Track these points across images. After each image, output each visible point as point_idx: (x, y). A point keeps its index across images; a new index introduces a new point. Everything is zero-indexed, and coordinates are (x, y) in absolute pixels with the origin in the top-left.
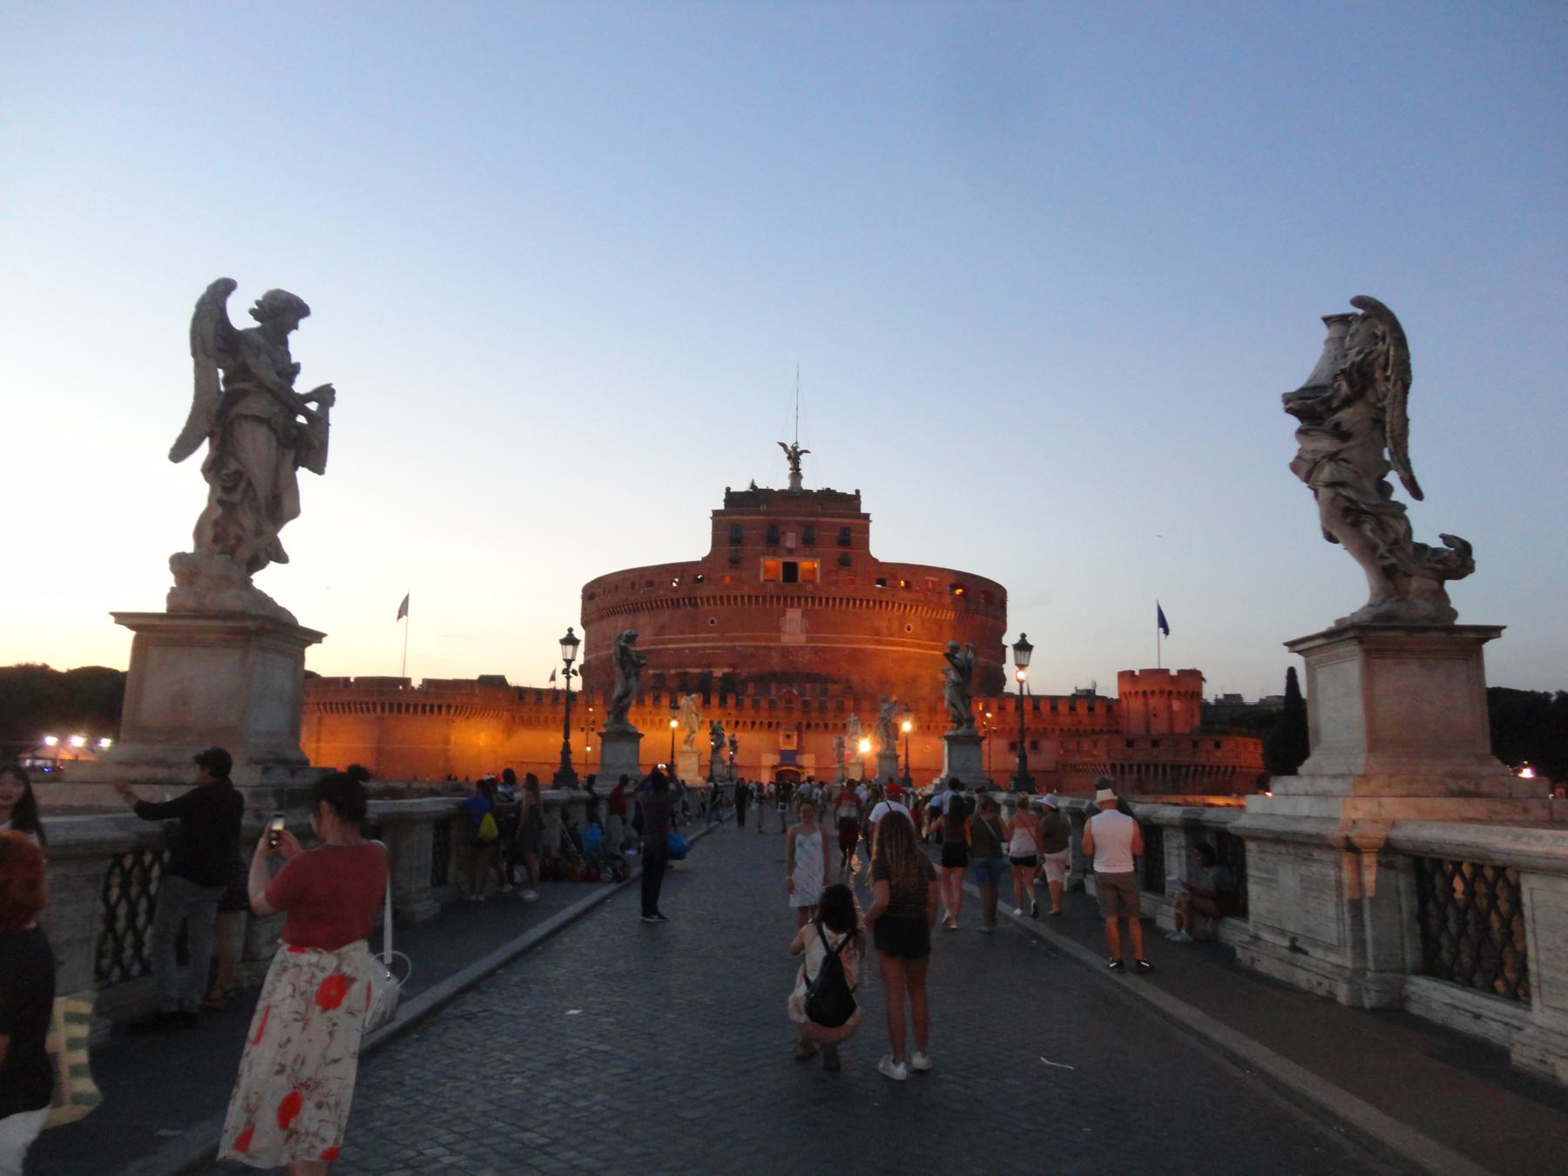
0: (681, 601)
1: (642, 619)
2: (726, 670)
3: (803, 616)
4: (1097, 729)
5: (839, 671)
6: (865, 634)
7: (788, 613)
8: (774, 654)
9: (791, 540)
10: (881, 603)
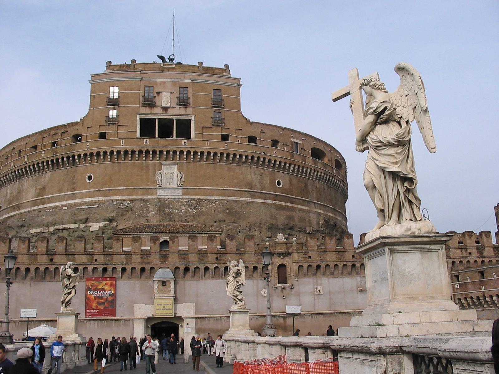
2: (102, 224)
3: (179, 170)
4: (487, 260)
5: (215, 222)
6: (240, 187)
7: (164, 167)
8: (151, 207)
9: (166, 100)
10: (253, 157)
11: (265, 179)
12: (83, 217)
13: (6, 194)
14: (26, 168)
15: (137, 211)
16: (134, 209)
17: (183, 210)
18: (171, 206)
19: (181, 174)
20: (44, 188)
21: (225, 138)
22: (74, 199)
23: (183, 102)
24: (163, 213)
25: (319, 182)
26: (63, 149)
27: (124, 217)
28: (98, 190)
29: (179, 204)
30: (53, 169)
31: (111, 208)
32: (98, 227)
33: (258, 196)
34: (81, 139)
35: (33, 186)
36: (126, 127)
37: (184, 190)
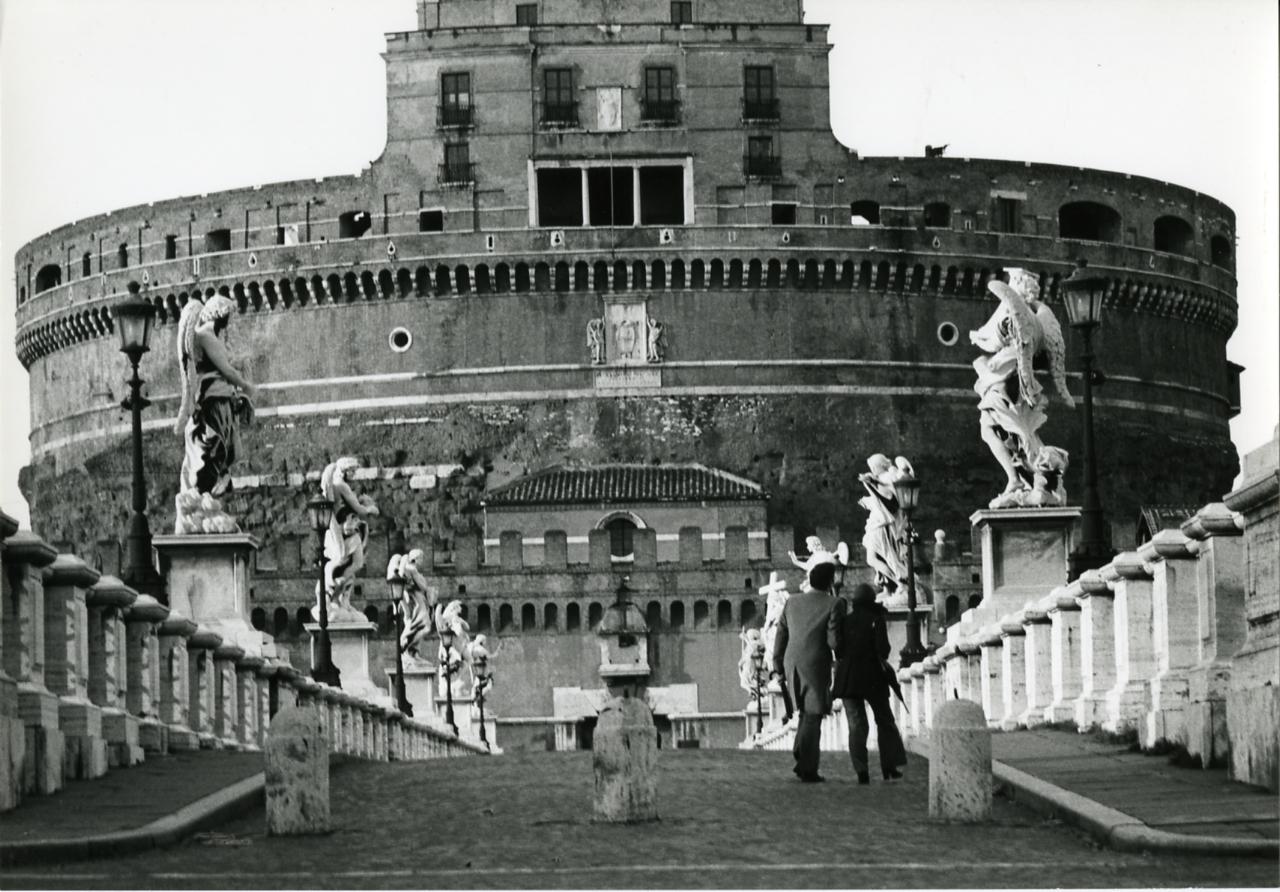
0: (309, 286)
2: (445, 471)
5: (757, 459)
12: (389, 451)
18: (631, 417)
19: (658, 325)
21: (784, 215)
26: (314, 254)
28: (430, 377)
30: (288, 305)
33: (881, 377)
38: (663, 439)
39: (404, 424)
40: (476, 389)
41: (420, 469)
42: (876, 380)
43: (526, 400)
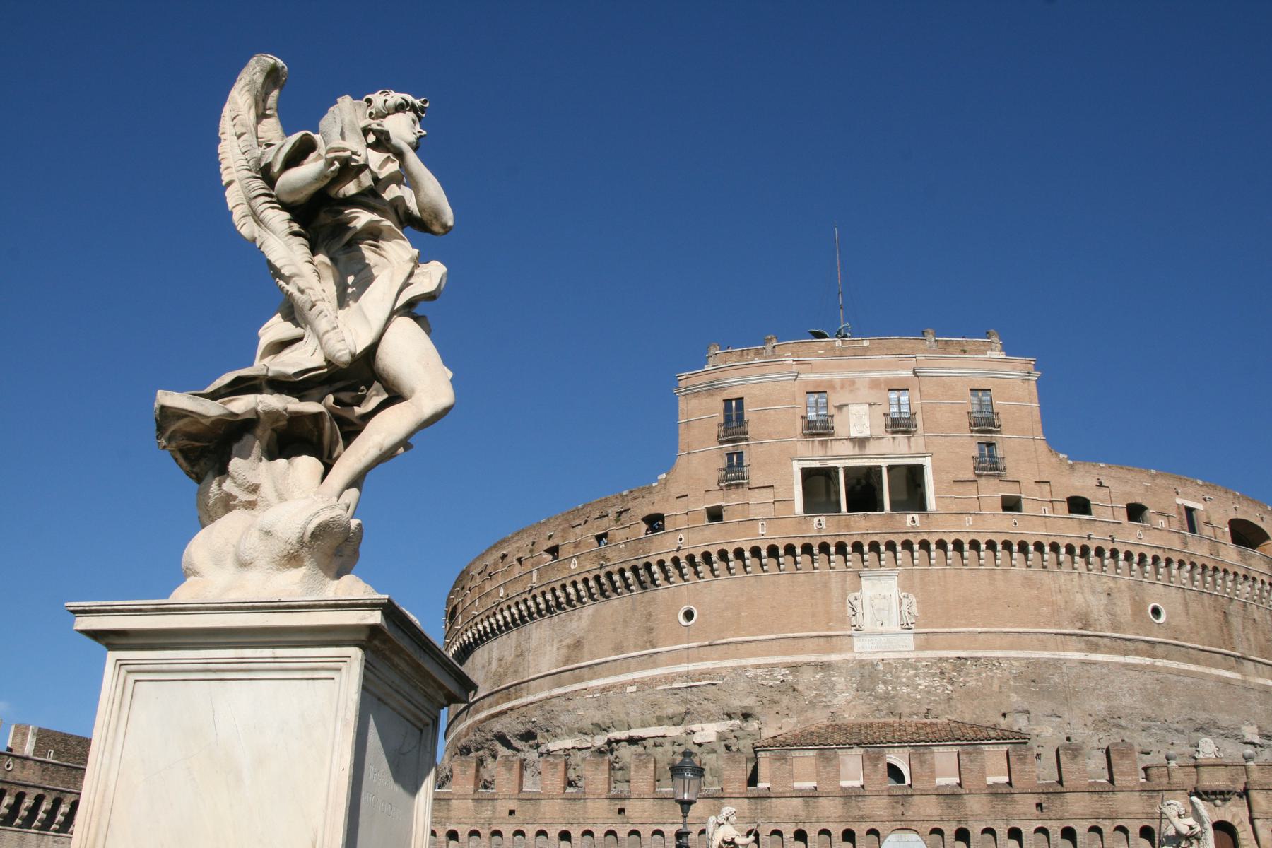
0: (616, 577)
1: (539, 631)
2: (724, 725)
3: (902, 587)
5: (1004, 715)
6: (1058, 625)
8: (840, 682)
11: (1120, 603)
13: (489, 659)
14: (534, 598)
15: (807, 693)
16: (799, 688)
17: (920, 687)
18: (889, 677)
20: (578, 644)
22: (652, 668)
23: (900, 426)
24: (871, 695)
25: (1258, 607)
26: (620, 551)
27: (776, 708)
28: (710, 645)
29: (908, 672)
31: (742, 685)
32: (715, 734)
33: (1105, 646)
34: (662, 528)
35: (553, 641)
36: (769, 490)
37: (918, 637)
38: (919, 697)
39: (691, 687)
40: (752, 655)
41: (703, 725)
42: (1102, 649)
43: (792, 663)
